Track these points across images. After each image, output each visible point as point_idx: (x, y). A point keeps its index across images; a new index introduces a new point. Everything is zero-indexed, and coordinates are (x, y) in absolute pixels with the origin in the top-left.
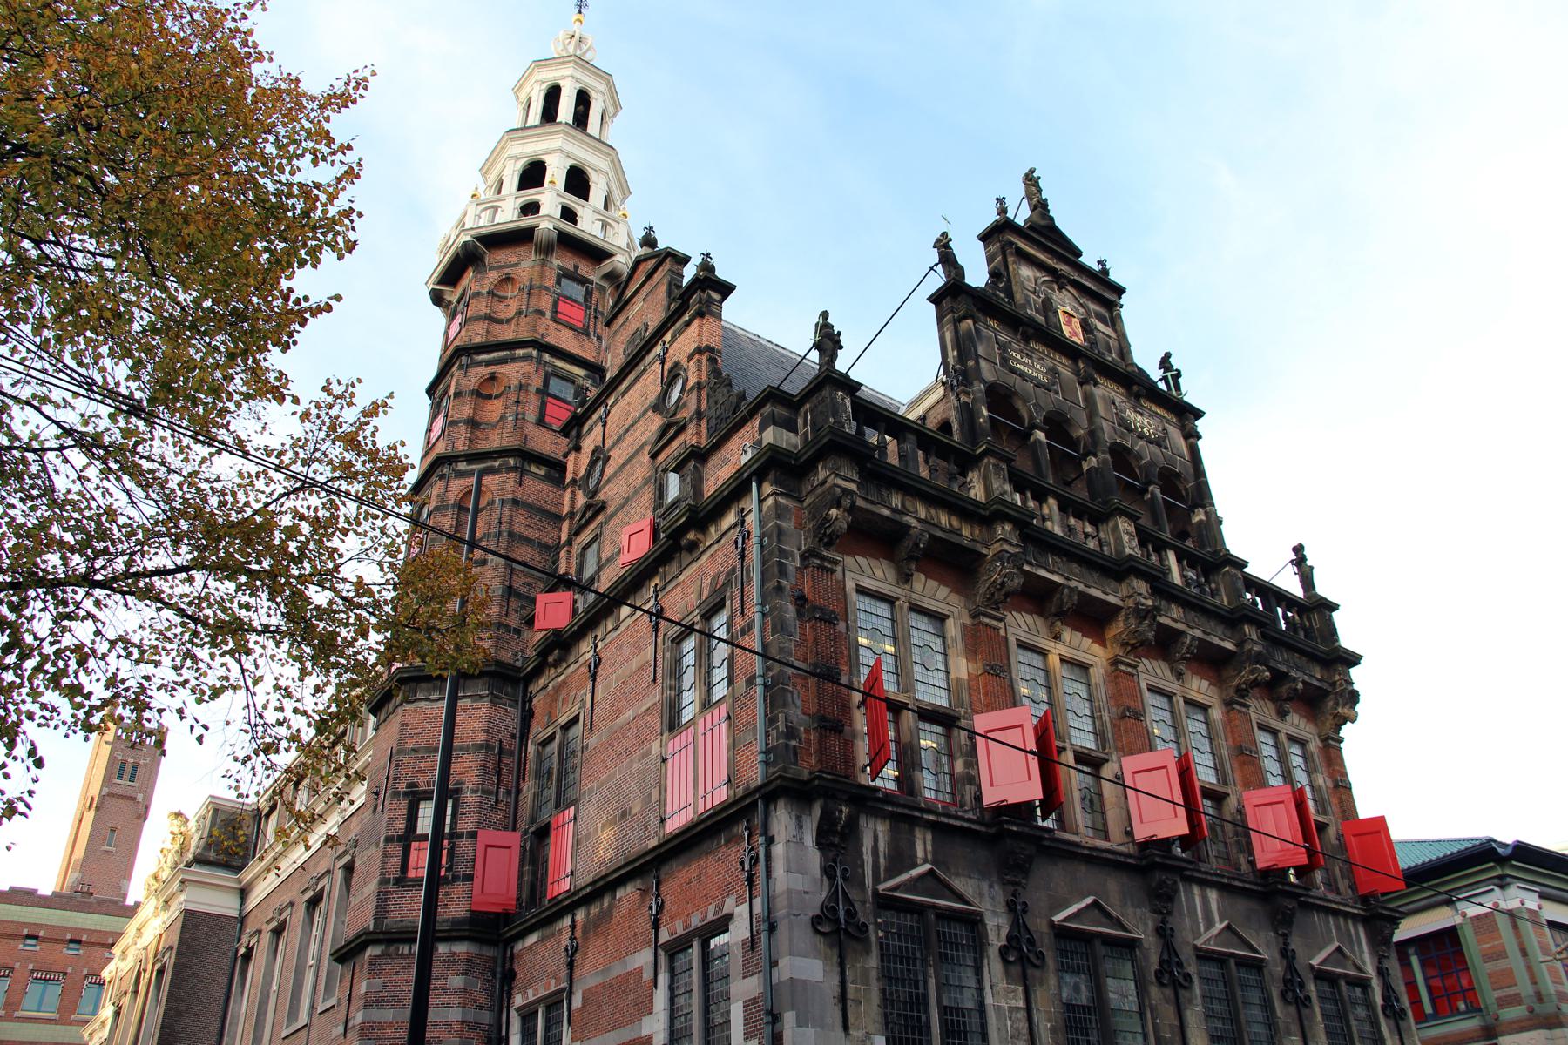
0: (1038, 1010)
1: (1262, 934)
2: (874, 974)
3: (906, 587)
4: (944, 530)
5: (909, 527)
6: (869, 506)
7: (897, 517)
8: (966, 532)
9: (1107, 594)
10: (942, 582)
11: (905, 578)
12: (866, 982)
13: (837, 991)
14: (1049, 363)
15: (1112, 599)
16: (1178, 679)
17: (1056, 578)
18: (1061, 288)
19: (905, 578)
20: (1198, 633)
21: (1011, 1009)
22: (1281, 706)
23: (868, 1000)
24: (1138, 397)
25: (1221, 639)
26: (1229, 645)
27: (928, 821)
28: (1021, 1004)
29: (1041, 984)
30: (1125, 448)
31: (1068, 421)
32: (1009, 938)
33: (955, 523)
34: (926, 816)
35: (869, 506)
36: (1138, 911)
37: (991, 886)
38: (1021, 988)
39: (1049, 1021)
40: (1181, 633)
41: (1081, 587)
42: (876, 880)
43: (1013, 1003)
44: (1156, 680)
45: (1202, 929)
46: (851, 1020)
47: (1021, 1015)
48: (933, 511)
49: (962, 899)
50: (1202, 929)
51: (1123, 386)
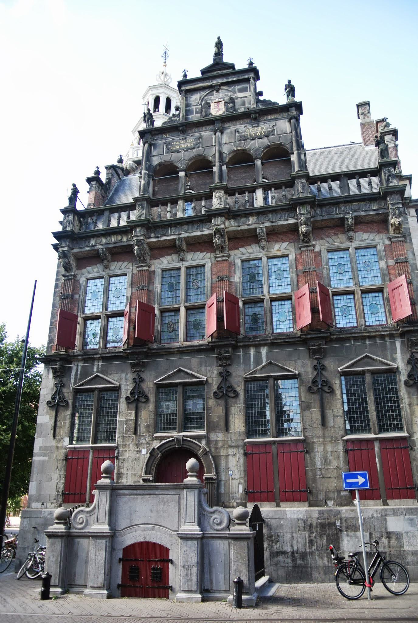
0: (141, 419)
1: (300, 362)
2: (68, 417)
3: (107, 270)
4: (113, 244)
5: (98, 250)
6: (81, 250)
7: (93, 248)
8: (125, 239)
9: (204, 231)
10: (124, 261)
11: (106, 267)
12: (65, 420)
13: (53, 425)
14: (197, 135)
15: (207, 232)
16: (263, 249)
17: (172, 237)
18: (218, 91)
19: (106, 267)
20: (267, 224)
21: (127, 421)
22: (347, 235)
23: (64, 426)
24: (255, 119)
25: (285, 220)
26: (292, 221)
27: (99, 358)
28: (133, 417)
29: (145, 408)
30: (243, 150)
31: (204, 157)
32: (132, 393)
33: (119, 238)
34: (95, 356)
35: (81, 250)
36: (209, 368)
37: (127, 374)
38: (133, 412)
39: (146, 422)
40: (255, 229)
41: (187, 235)
42: (75, 383)
43: (129, 418)
44: (248, 255)
45: (252, 368)
46: (57, 432)
47: (133, 423)
48: (108, 239)
49: (110, 383)
50: (252, 368)
51: (247, 118)
